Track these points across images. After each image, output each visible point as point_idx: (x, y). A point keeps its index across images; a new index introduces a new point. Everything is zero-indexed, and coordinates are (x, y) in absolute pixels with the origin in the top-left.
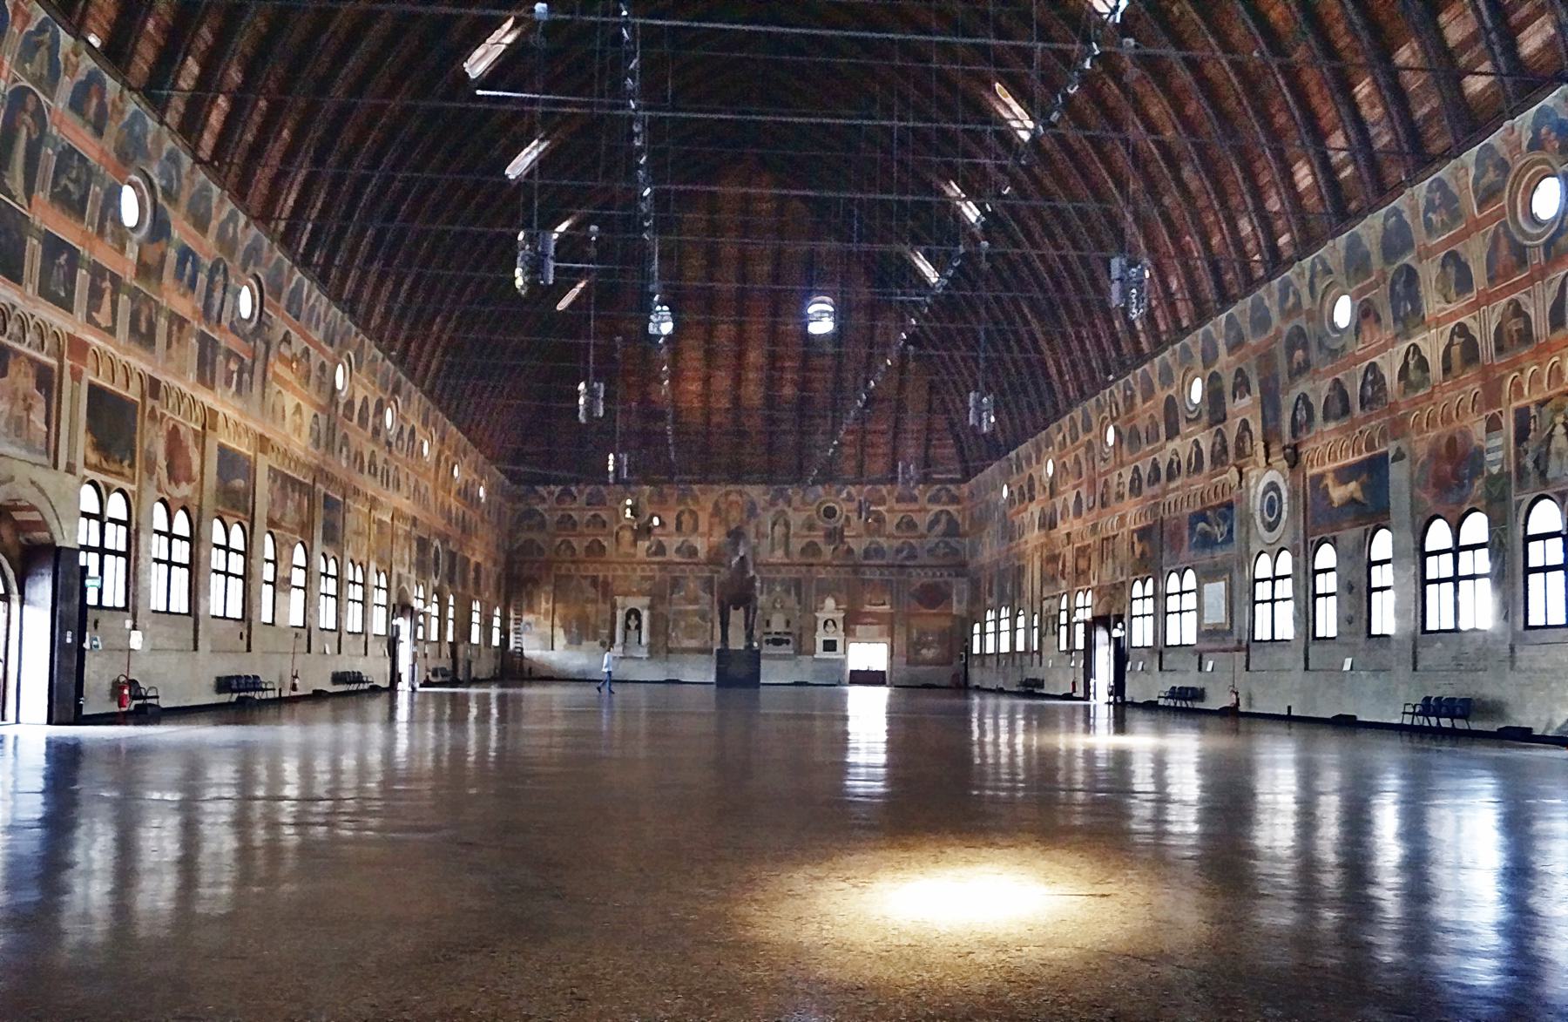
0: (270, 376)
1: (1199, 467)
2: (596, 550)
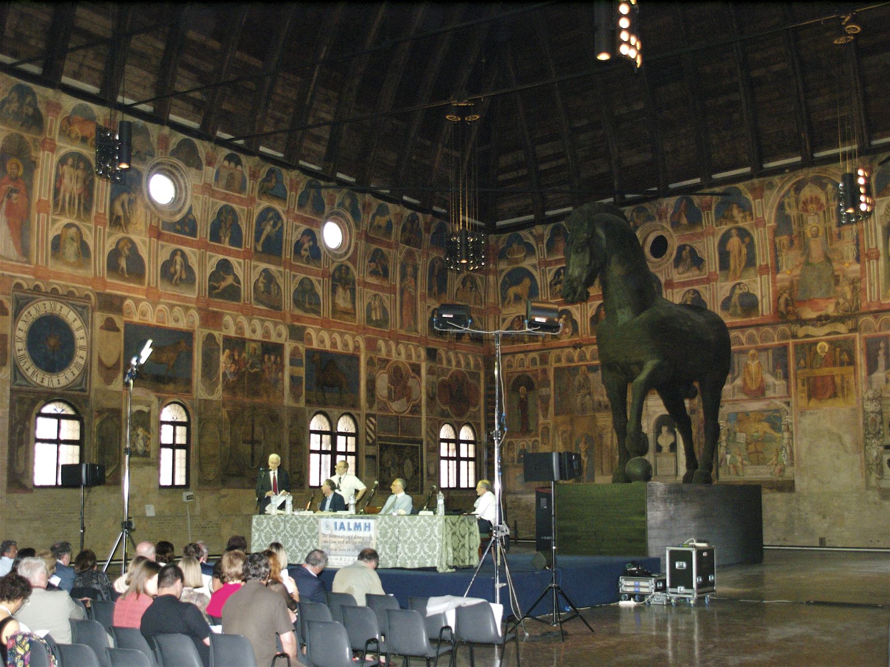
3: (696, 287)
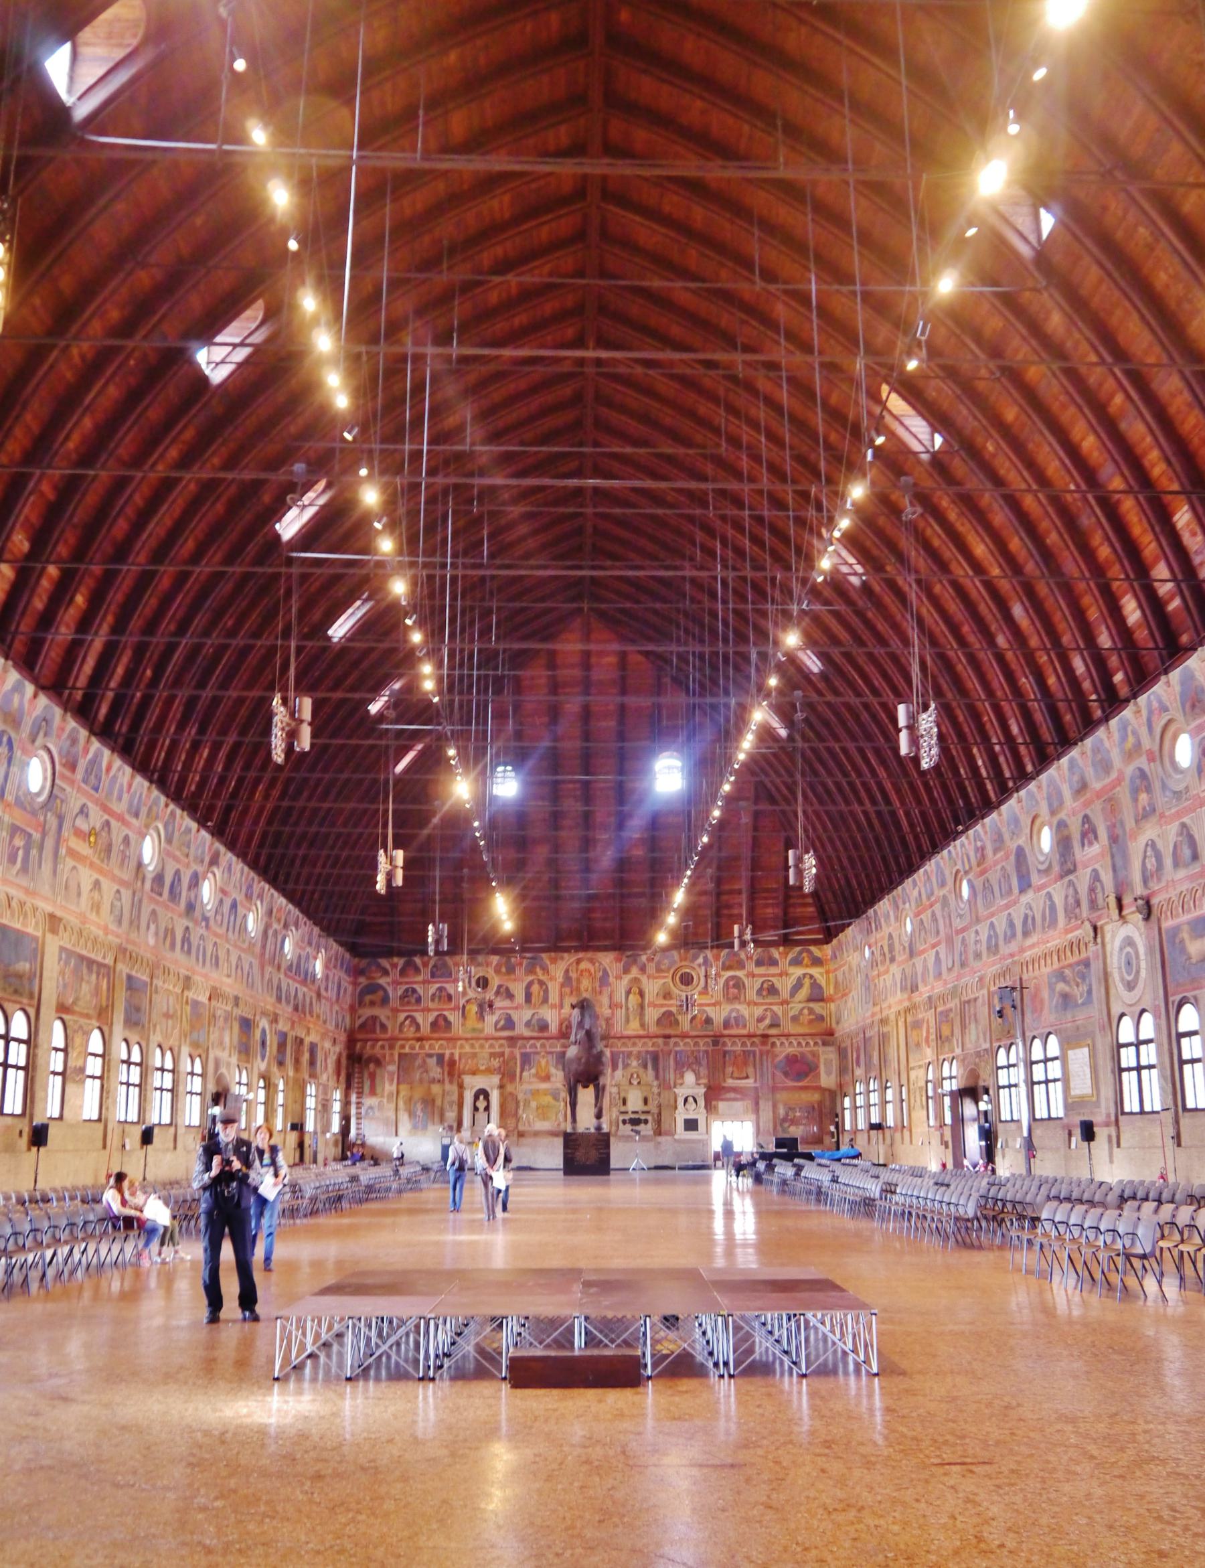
0: (63, 851)
1: (1054, 922)
2: (441, 1024)
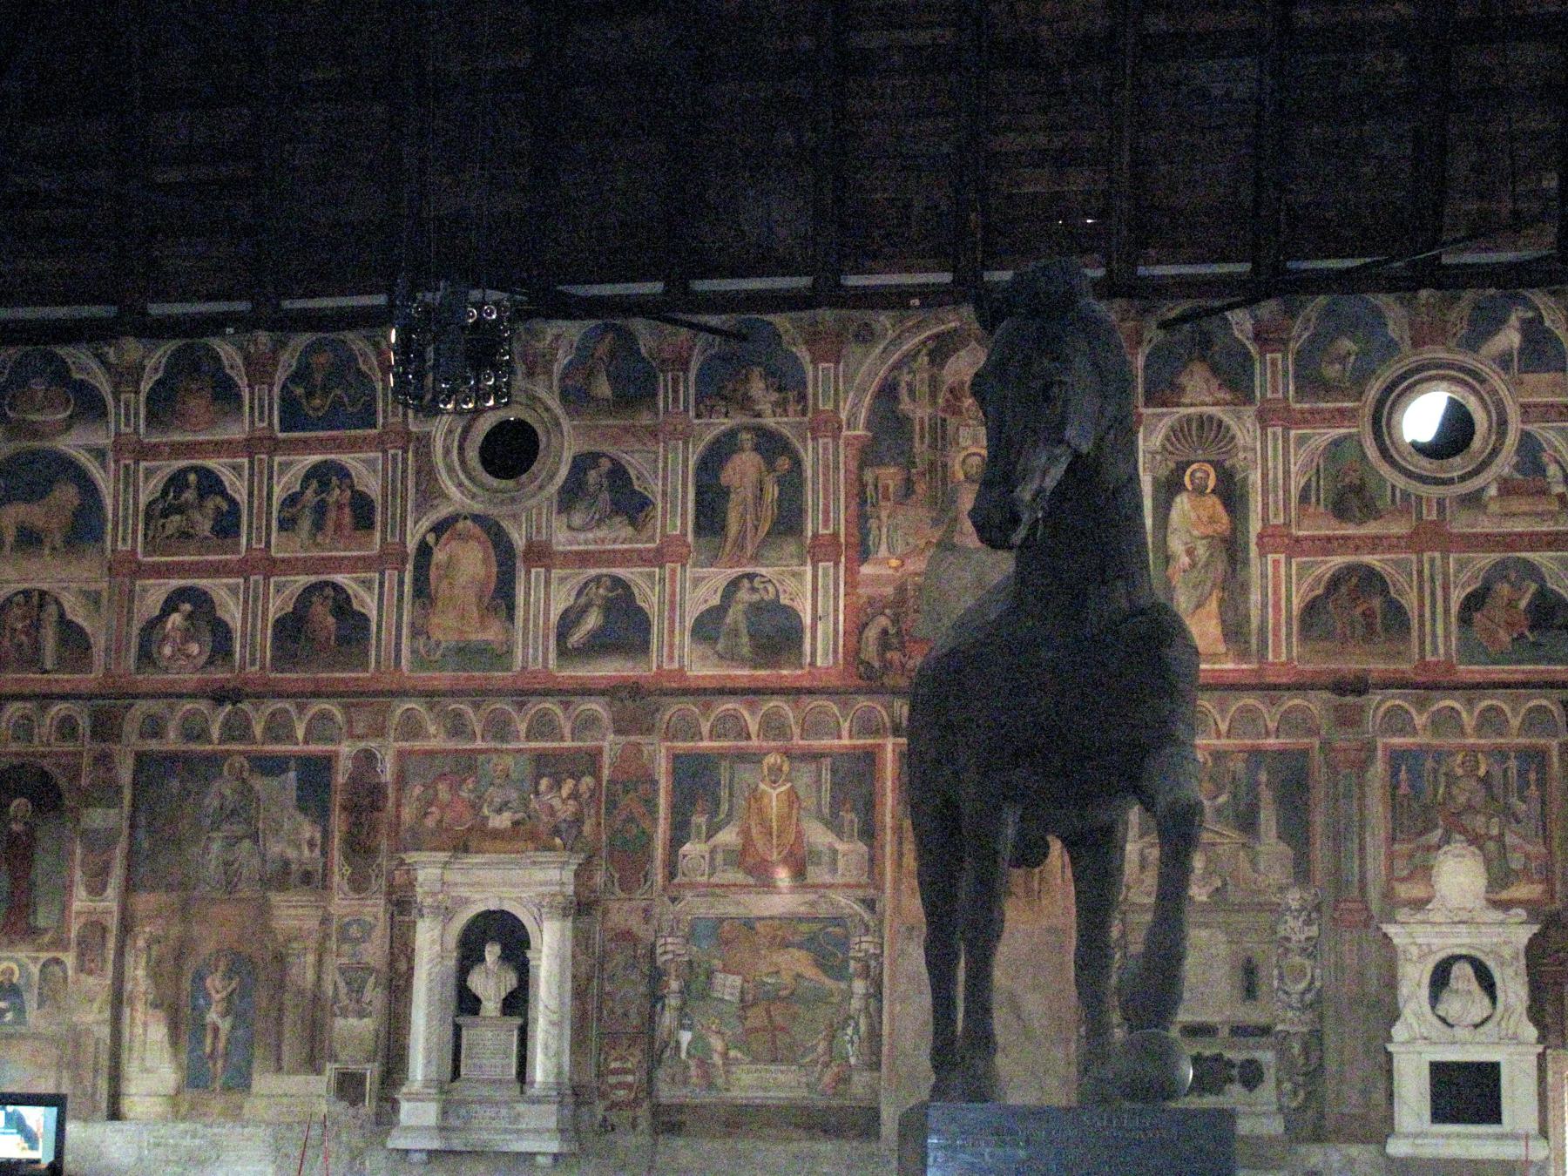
2: (321, 631)
3: (621, 572)
